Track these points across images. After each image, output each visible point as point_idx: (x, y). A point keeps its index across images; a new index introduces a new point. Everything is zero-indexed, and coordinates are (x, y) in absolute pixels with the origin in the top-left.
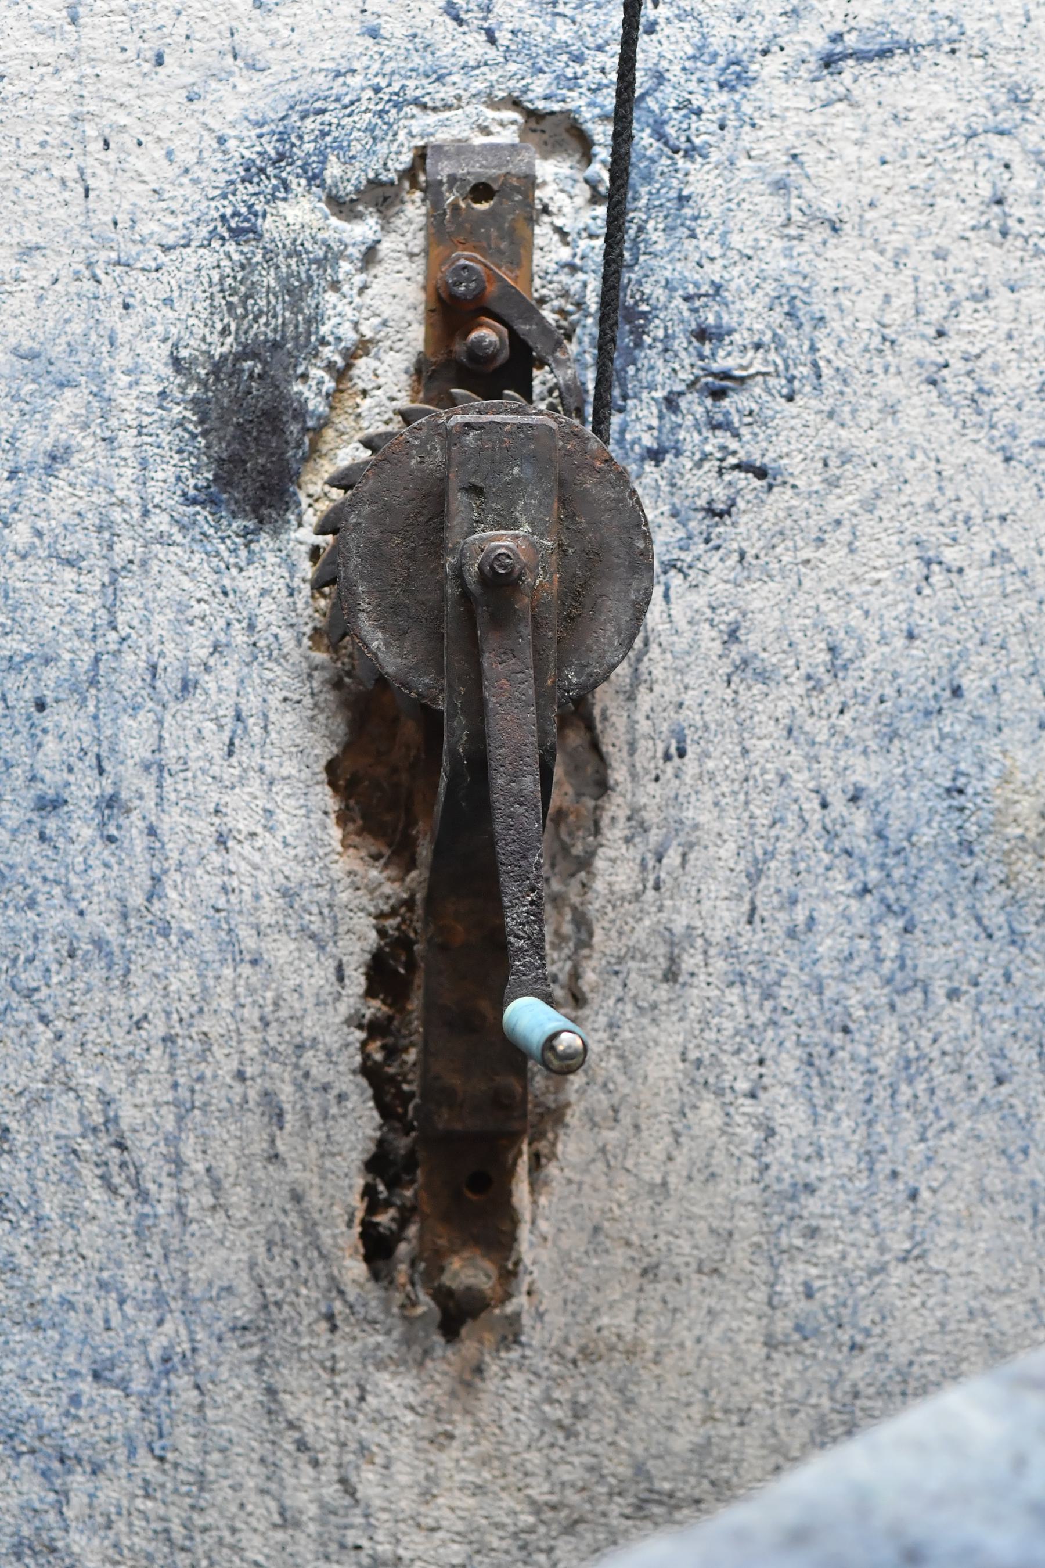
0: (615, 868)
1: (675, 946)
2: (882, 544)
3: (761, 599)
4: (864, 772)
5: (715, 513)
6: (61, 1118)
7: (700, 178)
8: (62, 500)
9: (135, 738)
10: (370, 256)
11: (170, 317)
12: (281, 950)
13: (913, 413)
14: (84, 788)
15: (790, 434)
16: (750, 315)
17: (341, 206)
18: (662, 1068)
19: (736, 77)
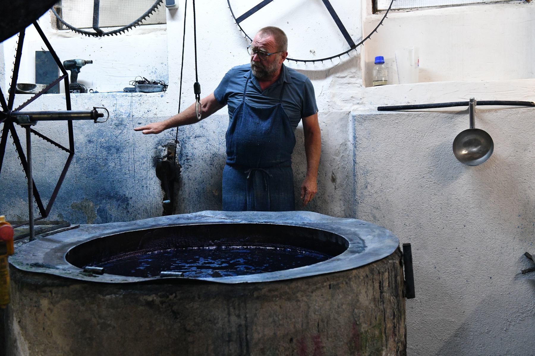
0: (180, 193)
1: (184, 198)
2: (198, 171)
3: (190, 174)
4: (197, 187)
5: (187, 168)
6: (143, 208)
7: (187, 145)
8: (144, 166)
9: (148, 182)
10: (165, 150)
11: (151, 154)
12: (157, 197)
13: (201, 162)
14: (145, 186)
15: (192, 163)
16: (190, 155)
17: (163, 147)
18: (183, 207)
19: (189, 138)
